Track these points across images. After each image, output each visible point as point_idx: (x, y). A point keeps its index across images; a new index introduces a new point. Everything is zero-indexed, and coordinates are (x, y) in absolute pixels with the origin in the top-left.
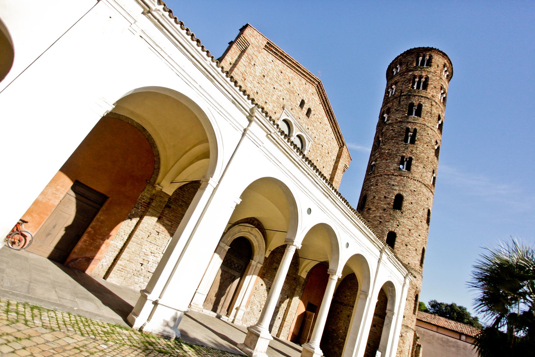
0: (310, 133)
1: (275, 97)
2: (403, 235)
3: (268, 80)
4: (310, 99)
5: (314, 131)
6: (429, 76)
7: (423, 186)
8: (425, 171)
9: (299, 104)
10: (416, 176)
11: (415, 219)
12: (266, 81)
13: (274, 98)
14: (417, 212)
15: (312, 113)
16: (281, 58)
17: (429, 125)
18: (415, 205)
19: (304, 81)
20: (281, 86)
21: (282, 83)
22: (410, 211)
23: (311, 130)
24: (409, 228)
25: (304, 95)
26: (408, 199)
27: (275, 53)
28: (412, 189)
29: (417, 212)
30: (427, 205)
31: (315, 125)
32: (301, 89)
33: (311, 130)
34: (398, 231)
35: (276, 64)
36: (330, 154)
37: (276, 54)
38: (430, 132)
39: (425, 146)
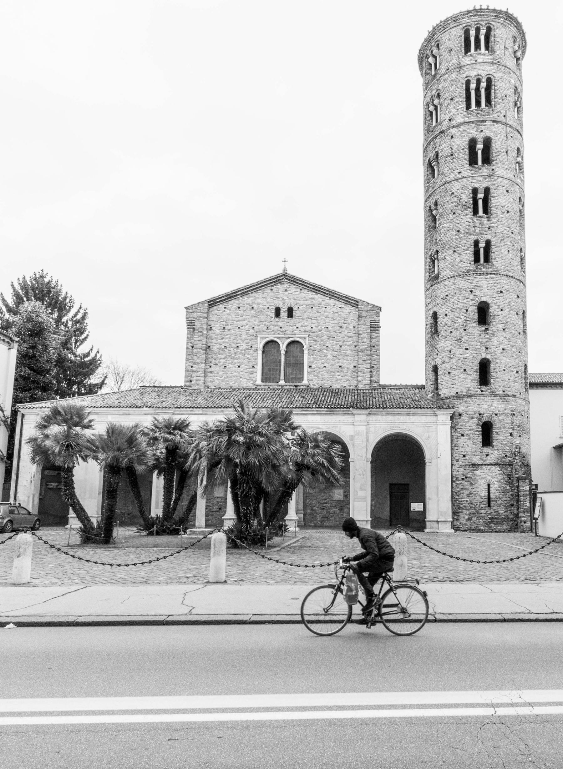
0: (302, 329)
1: (244, 334)
2: (444, 362)
3: (230, 327)
4: (285, 298)
5: (306, 324)
6: (440, 87)
7: (459, 279)
8: (456, 255)
9: (273, 315)
10: (445, 273)
11: (454, 332)
12: (229, 330)
13: (244, 335)
14: (454, 322)
15: (295, 308)
16: (230, 298)
17: (452, 176)
18: (451, 315)
19: (268, 290)
20: (244, 320)
21: (244, 317)
22: (446, 327)
23: (302, 326)
24: (449, 349)
25: (276, 302)
26: (441, 312)
27: (222, 301)
28: (443, 295)
29: (454, 322)
30: (472, 300)
31: (305, 316)
32: (268, 300)
33: (302, 326)
34: (438, 361)
35: (230, 306)
36: (344, 326)
37: (224, 300)
38: (456, 187)
39: (451, 216)
